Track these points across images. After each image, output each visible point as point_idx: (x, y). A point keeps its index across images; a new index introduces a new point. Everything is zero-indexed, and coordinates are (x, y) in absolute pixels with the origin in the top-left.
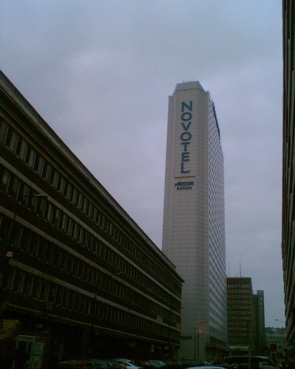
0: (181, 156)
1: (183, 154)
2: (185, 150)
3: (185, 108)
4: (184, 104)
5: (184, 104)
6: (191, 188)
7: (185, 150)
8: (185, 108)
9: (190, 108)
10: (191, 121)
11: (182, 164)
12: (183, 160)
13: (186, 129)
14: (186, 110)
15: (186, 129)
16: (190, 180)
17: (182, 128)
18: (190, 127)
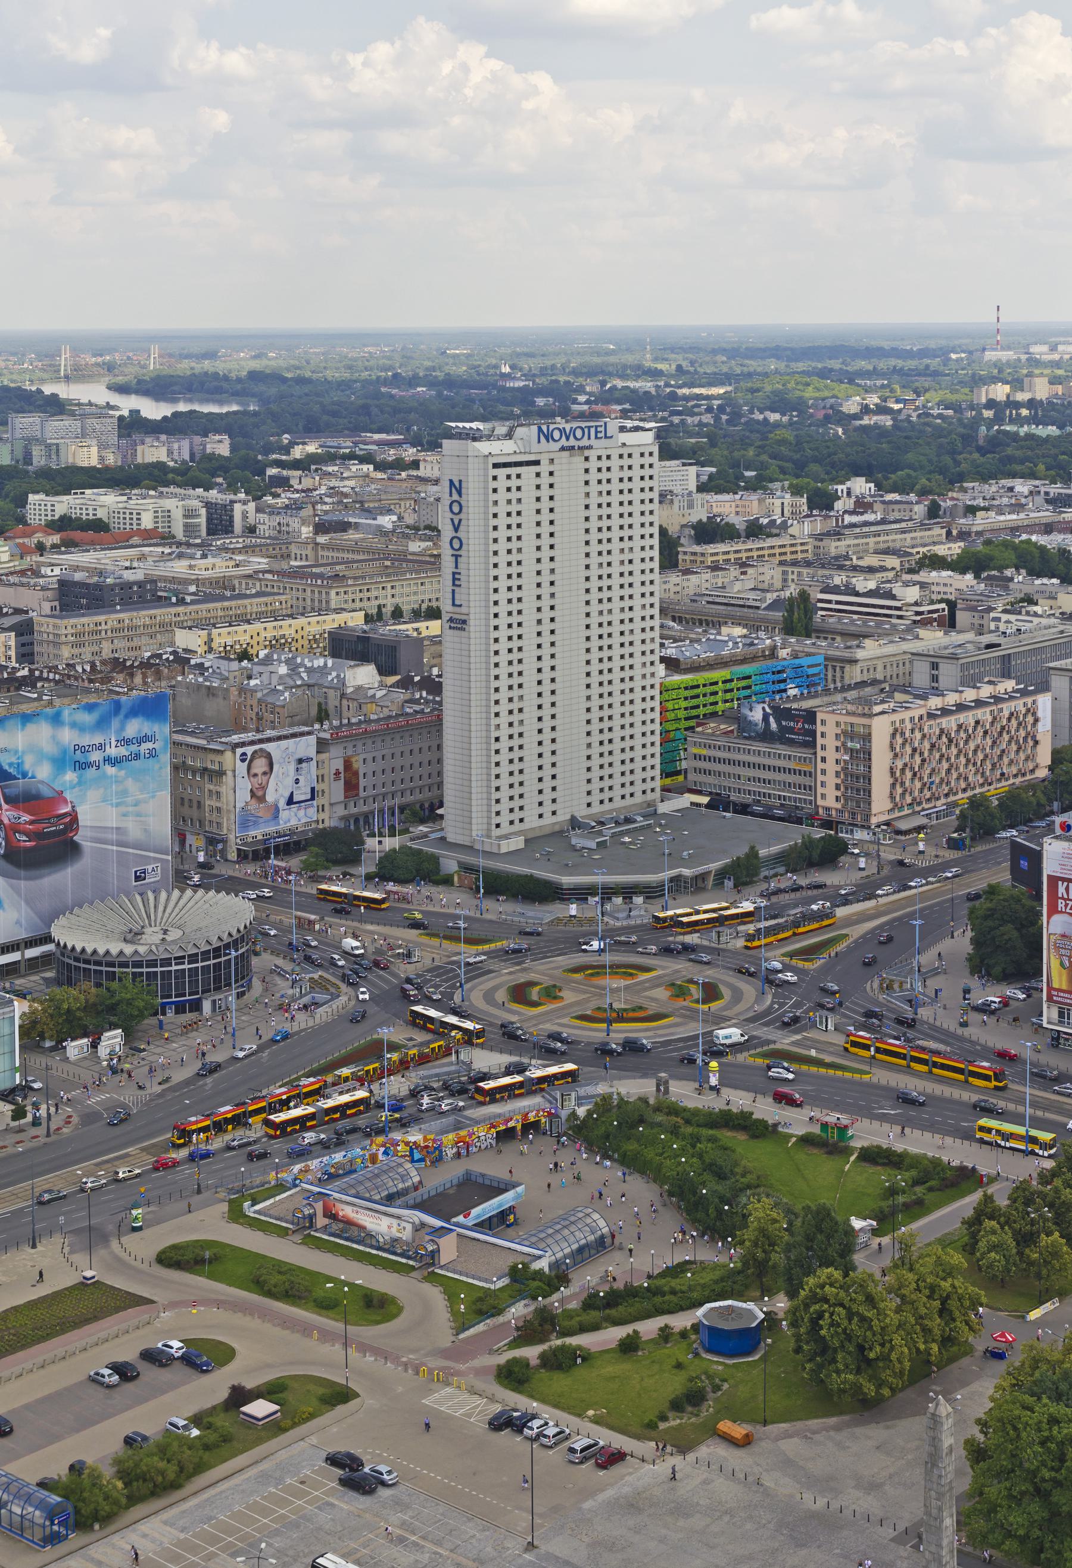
1: (454, 574)
4: (451, 481)
5: (451, 481)
9: (460, 494)
10: (462, 516)
13: (456, 530)
14: (455, 497)
15: (456, 530)
16: (464, 617)
17: (451, 527)
18: (462, 528)
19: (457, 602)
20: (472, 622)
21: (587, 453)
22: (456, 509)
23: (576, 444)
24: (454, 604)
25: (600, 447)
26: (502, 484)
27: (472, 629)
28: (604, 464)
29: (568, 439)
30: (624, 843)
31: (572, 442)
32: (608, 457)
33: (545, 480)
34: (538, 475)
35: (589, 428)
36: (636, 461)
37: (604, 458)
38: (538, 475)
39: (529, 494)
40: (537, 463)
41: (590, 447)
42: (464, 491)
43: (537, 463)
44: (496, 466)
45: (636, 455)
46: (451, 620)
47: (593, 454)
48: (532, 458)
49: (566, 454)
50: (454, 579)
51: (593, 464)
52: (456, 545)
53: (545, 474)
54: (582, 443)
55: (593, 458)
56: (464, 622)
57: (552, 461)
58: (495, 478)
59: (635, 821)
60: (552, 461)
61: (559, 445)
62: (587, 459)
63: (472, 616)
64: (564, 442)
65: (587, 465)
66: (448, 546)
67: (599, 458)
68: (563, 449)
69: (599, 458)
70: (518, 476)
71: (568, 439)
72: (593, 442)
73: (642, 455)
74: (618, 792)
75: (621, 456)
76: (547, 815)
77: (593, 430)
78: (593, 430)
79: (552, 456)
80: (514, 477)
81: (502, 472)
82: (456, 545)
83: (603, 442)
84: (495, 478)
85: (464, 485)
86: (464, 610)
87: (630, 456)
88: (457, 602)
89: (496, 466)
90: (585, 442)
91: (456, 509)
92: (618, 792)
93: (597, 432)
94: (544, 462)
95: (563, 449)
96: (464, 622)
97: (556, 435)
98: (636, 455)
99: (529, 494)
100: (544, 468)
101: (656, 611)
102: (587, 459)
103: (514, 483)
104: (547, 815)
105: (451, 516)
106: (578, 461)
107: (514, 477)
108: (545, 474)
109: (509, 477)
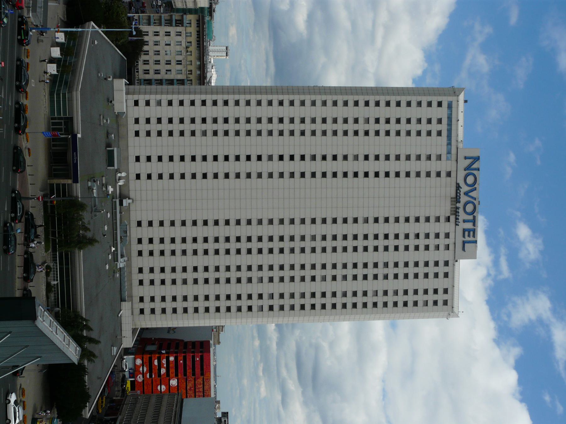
21: (452, 218)
29: (466, 194)
38: (439, 158)
47: (449, 227)
49: (454, 195)
51: (443, 227)
54: (461, 211)
64: (465, 188)
65: (442, 219)
68: (458, 187)
70: (439, 133)
71: (466, 194)
79: (453, 174)
81: (443, 113)
83: (460, 239)
84: (440, 104)
89: (450, 106)
90: (462, 216)
93: (469, 231)
95: (458, 187)
102: (448, 219)
106: (445, 209)
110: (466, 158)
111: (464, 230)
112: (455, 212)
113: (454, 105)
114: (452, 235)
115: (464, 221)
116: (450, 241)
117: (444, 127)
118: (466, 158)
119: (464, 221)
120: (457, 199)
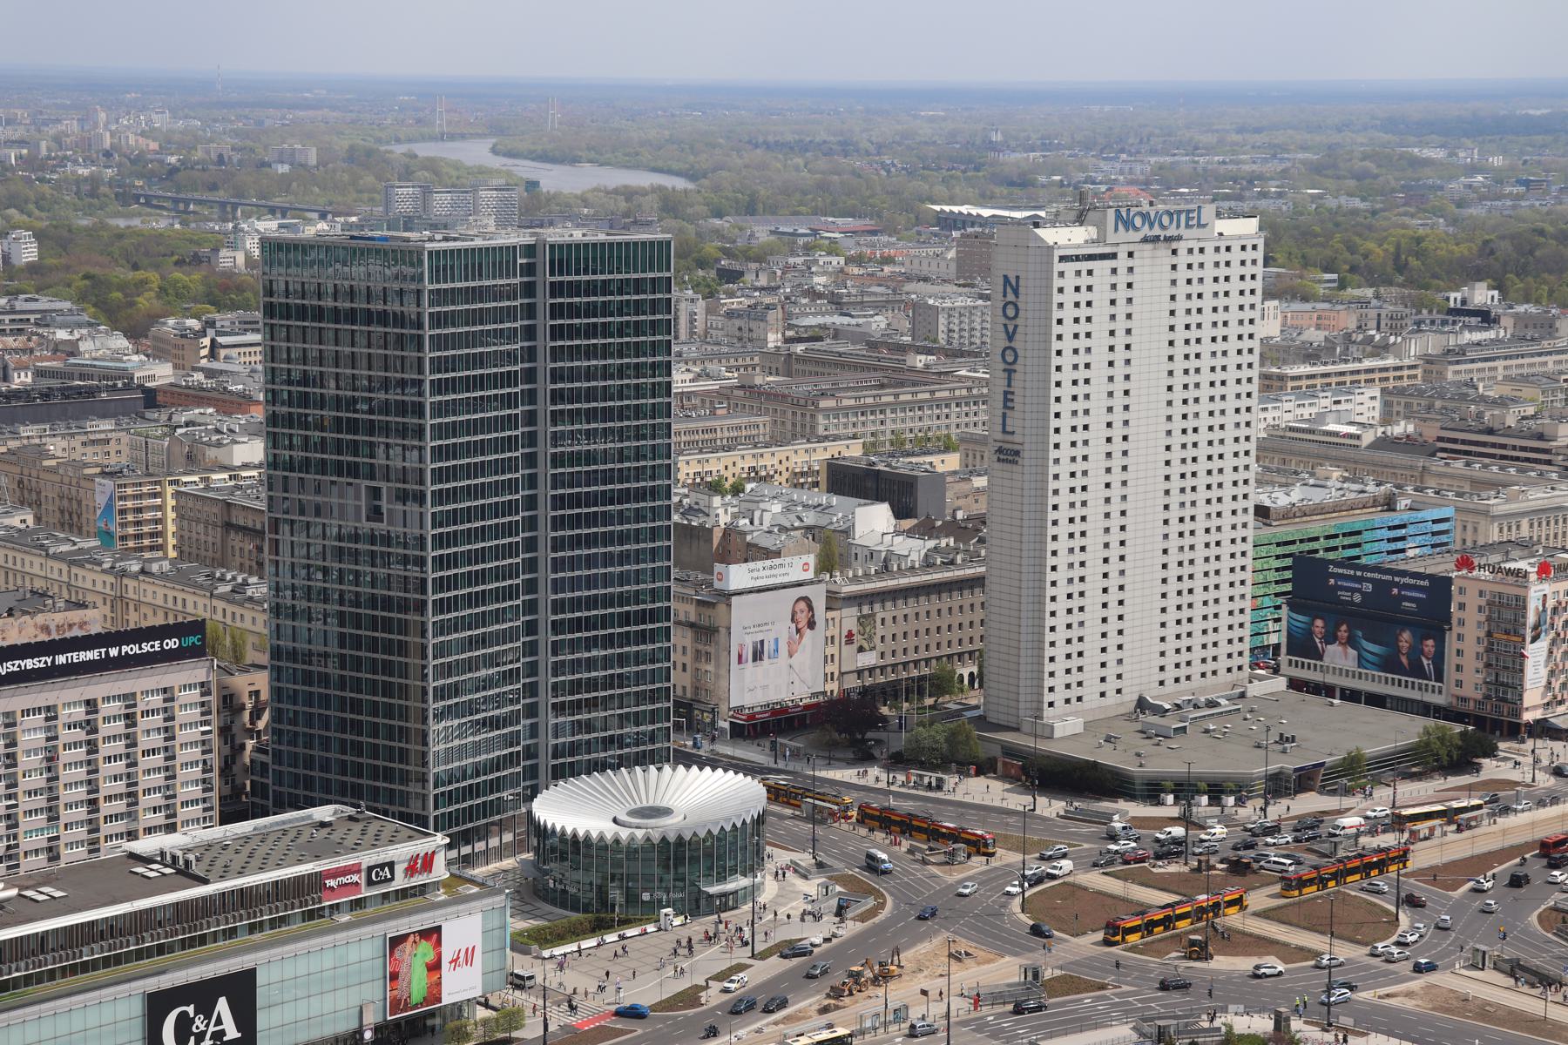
0: (1001, 398)
1: (1006, 393)
2: (1009, 385)
3: (1009, 290)
4: (1006, 277)
5: (1006, 277)
6: (1016, 463)
7: (1009, 385)
8: (1009, 290)
9: (1016, 292)
10: (1019, 321)
11: (1004, 416)
12: (1005, 407)
13: (1010, 338)
14: (1010, 297)
15: (1010, 338)
16: (1016, 447)
17: (1003, 335)
18: (1017, 337)
19: (1009, 429)
20: (1026, 454)
21: (1174, 245)
22: (1011, 312)
23: (1162, 234)
24: (1004, 431)
25: (1191, 238)
26: (1069, 282)
27: (1026, 462)
28: (1196, 259)
30: (1207, 731)
31: (1157, 231)
32: (1202, 250)
33: (1122, 279)
34: (1114, 271)
35: (1179, 213)
36: (1236, 256)
37: (1196, 251)
38: (1114, 271)
39: (1101, 296)
40: (1114, 256)
41: (1179, 238)
42: (1022, 290)
43: (1114, 256)
44: (1062, 259)
45: (1236, 248)
46: (1000, 450)
47: (1182, 247)
48: (1107, 250)
49: (1149, 246)
50: (1006, 400)
51: (1182, 259)
52: (1010, 359)
53: (1122, 271)
54: (1169, 233)
55: (1182, 252)
56: (1017, 453)
57: (1131, 255)
58: (1061, 274)
59: (1217, 705)
60: (1131, 255)
61: (1140, 235)
62: (1174, 252)
63: (1027, 447)
66: (999, 358)
67: (1190, 251)
68: (1145, 240)
69: (1190, 251)
70: (1090, 273)
71: (1151, 226)
72: (1183, 231)
73: (1243, 248)
74: (1197, 668)
75: (1217, 249)
76: (1111, 693)
77: (1183, 217)
78: (1183, 217)
80: (1084, 273)
81: (1069, 268)
82: (1010, 359)
83: (1195, 232)
85: (1022, 282)
86: (1017, 438)
87: (1228, 249)
88: (1009, 429)
89: (1062, 259)
90: (1172, 232)
91: (1011, 312)
92: (1197, 668)
93: (1188, 219)
94: (1122, 255)
95: (1145, 240)
96: (1017, 453)
97: (1138, 221)
98: (1236, 248)
99: (1101, 296)
100: (1122, 263)
101: (1252, 446)
102: (1174, 252)
103: (1084, 281)
104: (1111, 693)
105: (1003, 320)
107: (1084, 273)
108: (1122, 271)
109: (1078, 273)
110: (1116, 229)
111: (1188, 226)
112: (1169, 239)
113: (1063, 252)
114: (1191, 244)
115: (1178, 226)
116: (1196, 246)
117: (1084, 266)
118: (1116, 229)
119: (1178, 226)
120: (1156, 239)
